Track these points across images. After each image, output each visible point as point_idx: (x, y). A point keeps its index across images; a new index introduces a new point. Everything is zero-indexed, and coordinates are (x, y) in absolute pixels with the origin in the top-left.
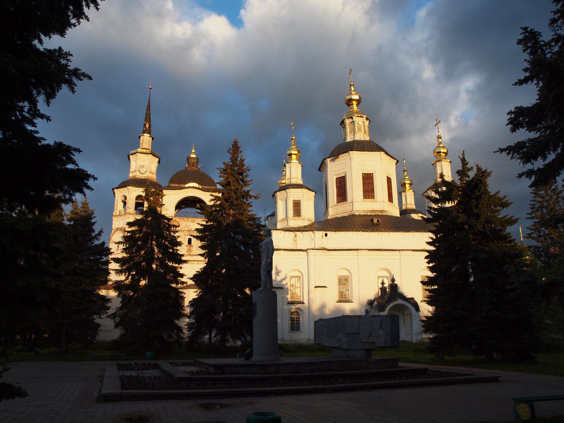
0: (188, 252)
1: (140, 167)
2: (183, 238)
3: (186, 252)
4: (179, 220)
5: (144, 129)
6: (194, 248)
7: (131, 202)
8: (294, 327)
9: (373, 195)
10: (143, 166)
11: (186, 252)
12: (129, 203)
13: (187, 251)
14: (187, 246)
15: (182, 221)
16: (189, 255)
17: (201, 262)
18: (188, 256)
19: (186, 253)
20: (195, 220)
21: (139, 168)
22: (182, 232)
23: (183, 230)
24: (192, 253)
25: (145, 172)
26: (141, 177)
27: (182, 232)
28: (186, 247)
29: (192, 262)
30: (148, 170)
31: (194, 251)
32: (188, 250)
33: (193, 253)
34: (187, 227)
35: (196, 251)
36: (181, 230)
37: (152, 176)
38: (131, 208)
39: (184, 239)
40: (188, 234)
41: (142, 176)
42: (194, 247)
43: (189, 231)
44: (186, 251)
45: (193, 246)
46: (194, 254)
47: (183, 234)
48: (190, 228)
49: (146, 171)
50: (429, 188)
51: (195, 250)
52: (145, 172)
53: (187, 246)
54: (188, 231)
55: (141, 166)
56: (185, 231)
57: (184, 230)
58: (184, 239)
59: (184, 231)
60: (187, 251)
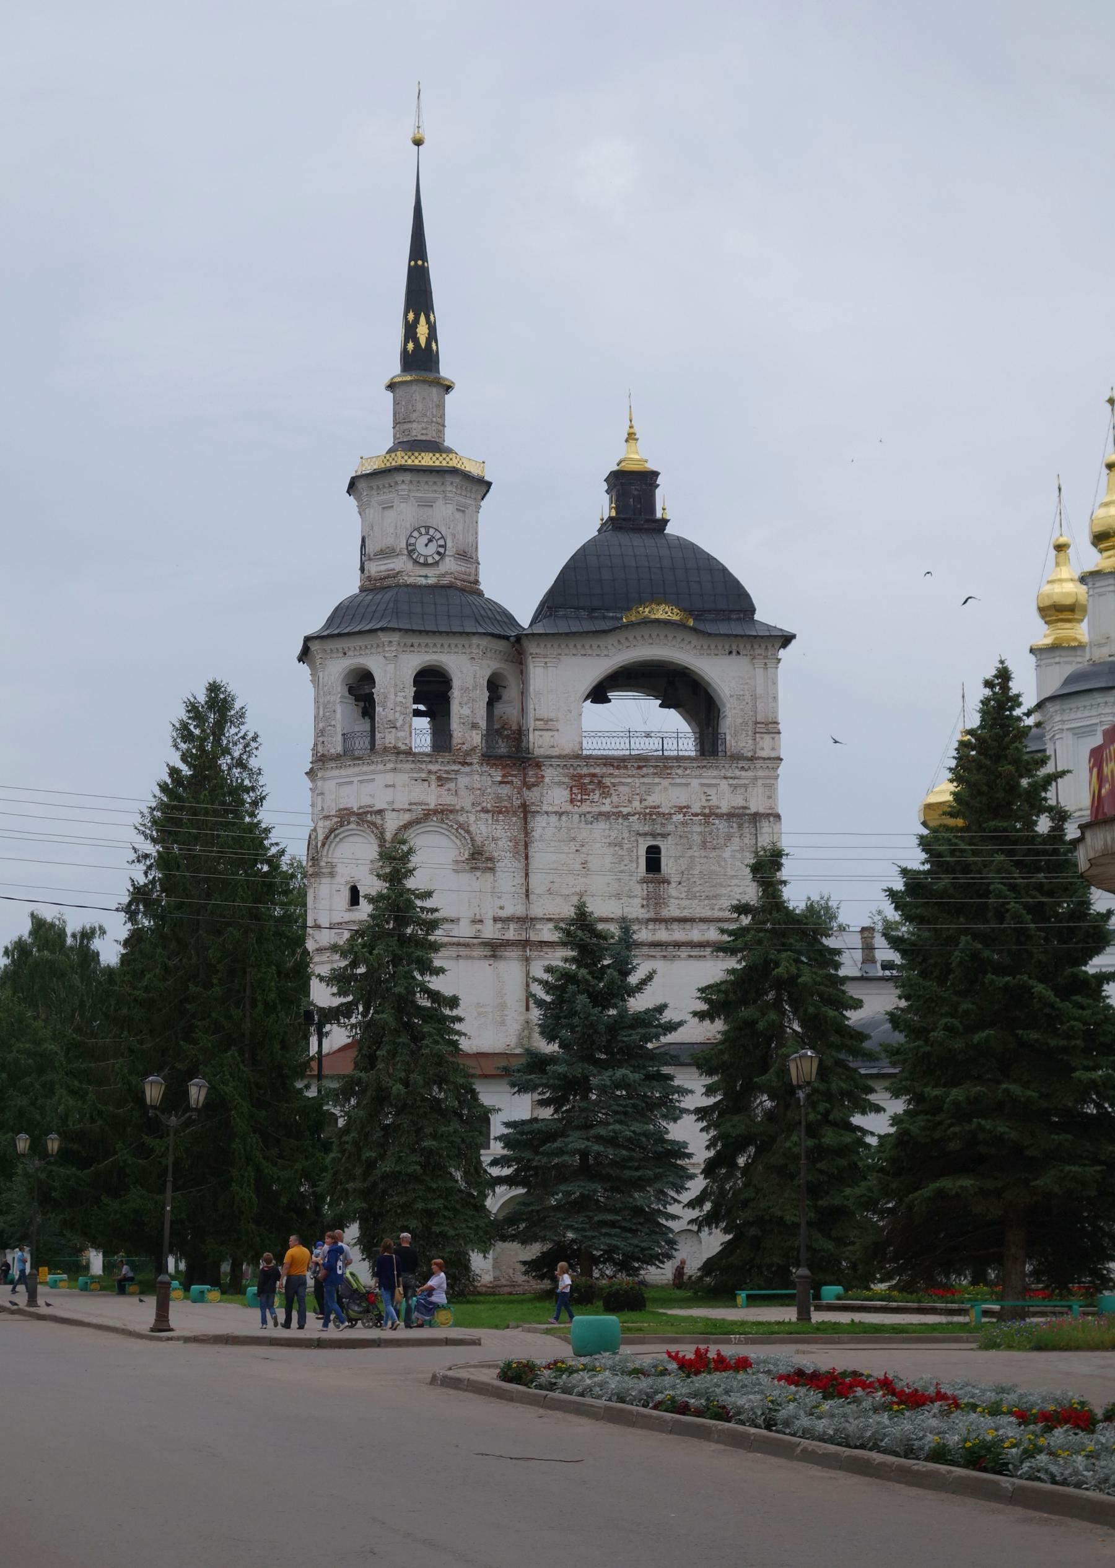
0: (648, 906)
1: (416, 534)
2: (626, 847)
3: (643, 906)
4: (604, 770)
5: (410, 346)
6: (672, 890)
7: (399, 699)
10: (427, 528)
11: (643, 906)
12: (390, 705)
13: (645, 903)
14: (644, 881)
15: (616, 772)
19: (643, 910)
20: (671, 767)
21: (412, 541)
22: (620, 821)
23: (625, 811)
24: (666, 913)
25: (437, 557)
26: (423, 581)
27: (620, 821)
28: (639, 887)
29: (670, 949)
30: (449, 544)
32: (648, 899)
33: (672, 910)
35: (686, 903)
36: (614, 814)
37: (463, 569)
38: (398, 725)
39: (630, 850)
40: (647, 829)
41: (426, 577)
42: (673, 885)
45: (669, 883)
46: (676, 913)
48: (652, 800)
49: (442, 550)
52: (439, 553)
53: (644, 881)
54: (646, 814)
55: (418, 529)
57: (629, 814)
58: (630, 850)
59: (626, 817)
60: (645, 903)
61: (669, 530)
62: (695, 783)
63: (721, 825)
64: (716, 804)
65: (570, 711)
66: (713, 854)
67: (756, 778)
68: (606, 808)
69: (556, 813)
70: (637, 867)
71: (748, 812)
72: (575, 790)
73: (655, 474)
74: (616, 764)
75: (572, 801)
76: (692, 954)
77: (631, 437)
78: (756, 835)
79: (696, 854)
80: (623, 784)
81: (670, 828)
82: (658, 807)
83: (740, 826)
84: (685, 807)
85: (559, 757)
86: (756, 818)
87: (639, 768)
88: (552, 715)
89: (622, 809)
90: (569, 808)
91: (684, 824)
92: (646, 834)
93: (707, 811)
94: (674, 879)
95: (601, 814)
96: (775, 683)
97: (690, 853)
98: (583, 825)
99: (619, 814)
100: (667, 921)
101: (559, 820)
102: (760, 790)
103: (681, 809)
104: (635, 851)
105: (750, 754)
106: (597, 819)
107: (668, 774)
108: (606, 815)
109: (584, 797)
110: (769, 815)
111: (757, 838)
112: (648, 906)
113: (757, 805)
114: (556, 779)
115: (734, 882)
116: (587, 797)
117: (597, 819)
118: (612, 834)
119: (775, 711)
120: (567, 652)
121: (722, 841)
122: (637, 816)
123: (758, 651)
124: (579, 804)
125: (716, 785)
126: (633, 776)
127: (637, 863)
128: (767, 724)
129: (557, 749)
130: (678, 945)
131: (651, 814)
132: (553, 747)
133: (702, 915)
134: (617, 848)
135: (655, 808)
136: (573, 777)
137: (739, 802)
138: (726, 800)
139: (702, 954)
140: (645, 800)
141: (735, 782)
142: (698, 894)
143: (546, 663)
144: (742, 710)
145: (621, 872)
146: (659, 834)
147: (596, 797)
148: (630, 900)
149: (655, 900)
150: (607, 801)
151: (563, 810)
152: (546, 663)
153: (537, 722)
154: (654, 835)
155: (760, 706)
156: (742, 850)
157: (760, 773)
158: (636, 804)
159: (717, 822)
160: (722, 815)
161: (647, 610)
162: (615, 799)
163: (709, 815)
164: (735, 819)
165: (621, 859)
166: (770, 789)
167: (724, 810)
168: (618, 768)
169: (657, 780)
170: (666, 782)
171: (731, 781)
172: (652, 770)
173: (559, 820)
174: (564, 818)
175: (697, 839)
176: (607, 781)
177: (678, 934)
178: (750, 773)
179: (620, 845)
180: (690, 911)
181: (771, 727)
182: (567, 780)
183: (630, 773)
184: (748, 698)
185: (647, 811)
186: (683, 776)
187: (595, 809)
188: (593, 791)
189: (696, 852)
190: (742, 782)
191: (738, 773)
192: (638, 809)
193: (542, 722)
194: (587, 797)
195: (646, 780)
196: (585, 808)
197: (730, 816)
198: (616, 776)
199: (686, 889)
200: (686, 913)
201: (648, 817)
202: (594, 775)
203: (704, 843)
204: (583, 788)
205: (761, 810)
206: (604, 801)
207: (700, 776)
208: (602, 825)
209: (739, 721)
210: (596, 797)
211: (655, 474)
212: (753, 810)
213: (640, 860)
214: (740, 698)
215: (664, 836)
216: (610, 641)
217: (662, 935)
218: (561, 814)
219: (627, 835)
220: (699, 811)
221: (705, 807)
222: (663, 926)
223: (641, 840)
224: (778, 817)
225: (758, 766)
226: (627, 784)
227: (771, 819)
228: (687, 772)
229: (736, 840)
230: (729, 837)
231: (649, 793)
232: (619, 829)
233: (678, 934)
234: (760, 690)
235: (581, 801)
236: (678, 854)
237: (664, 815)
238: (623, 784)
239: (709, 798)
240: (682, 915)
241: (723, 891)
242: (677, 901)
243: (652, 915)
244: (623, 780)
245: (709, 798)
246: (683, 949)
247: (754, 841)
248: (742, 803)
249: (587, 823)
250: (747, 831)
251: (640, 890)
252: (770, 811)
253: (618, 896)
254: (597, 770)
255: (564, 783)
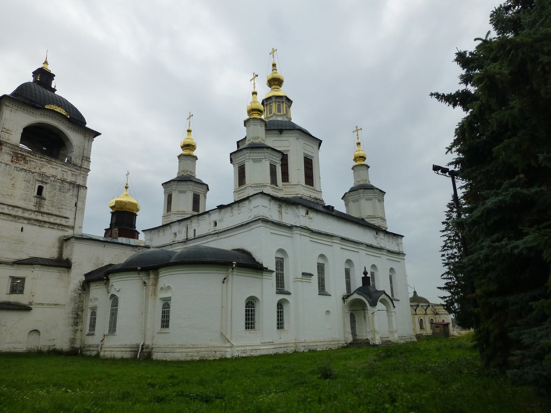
0: (36, 206)
2: (31, 183)
3: (34, 206)
4: (27, 154)
6: (46, 202)
8: (249, 323)
9: (312, 181)
11: (34, 206)
13: (35, 204)
14: (35, 197)
15: (32, 156)
16: (38, 212)
17: (56, 226)
18: (36, 213)
19: (34, 207)
22: (30, 173)
23: (33, 171)
24: (42, 210)
27: (30, 173)
28: (34, 198)
31: (45, 206)
32: (36, 204)
33: (44, 210)
34: (38, 168)
36: (28, 170)
39: (32, 185)
40: (40, 179)
43: (42, 175)
44: (32, 204)
45: (45, 200)
46: (46, 211)
47: (32, 177)
48: (43, 170)
50: (351, 188)
51: (48, 206)
53: (35, 197)
54: (40, 174)
56: (36, 173)
57: (34, 172)
59: (33, 173)
60: (35, 204)
61: (56, 93)
62: (60, 169)
63: (67, 186)
64: (66, 178)
65: (17, 130)
66: (63, 194)
67: (81, 174)
68: (26, 168)
69: (5, 164)
70: (34, 191)
71: (76, 183)
72: (14, 158)
73: (54, 75)
74: (32, 154)
75: (12, 161)
76: (50, 226)
77: (46, 63)
78: (78, 191)
79: (56, 192)
80: (33, 161)
81: (49, 181)
82: (45, 173)
83: (73, 187)
84: (55, 176)
85: (10, 144)
86: (79, 186)
87: (41, 158)
88: (10, 129)
89: (32, 170)
90: (11, 163)
91: (54, 181)
92: (39, 181)
93: (62, 179)
94: (47, 198)
95: (23, 169)
96: (91, 146)
97: (55, 191)
98: (15, 171)
99: (30, 171)
100: (43, 213)
101: (6, 166)
102: (82, 178)
103: (53, 176)
104: (34, 186)
105: (80, 166)
106: (21, 170)
107: (51, 163)
108: (26, 170)
109: (17, 161)
110: (83, 186)
111: (78, 193)
112: (36, 206)
113: (79, 182)
114: (7, 152)
115: (69, 205)
116: (18, 162)
117: (21, 170)
118: (26, 177)
119: (90, 155)
120: (20, 110)
121: (66, 190)
122: (37, 174)
123: (87, 135)
124: (15, 163)
125: (67, 172)
126: (38, 160)
127: (35, 190)
128: (87, 158)
129: (10, 141)
130: (45, 222)
131: (42, 175)
132: (9, 140)
133: (56, 214)
134: (27, 183)
135: (44, 173)
136: (14, 153)
137: (73, 179)
138: (70, 178)
139: (53, 227)
140: (41, 169)
141: (73, 173)
142: (55, 206)
143: (11, 110)
144: (79, 151)
145: (27, 191)
146: (44, 182)
147: (22, 163)
148: (29, 202)
149: (39, 204)
150: (27, 165)
151: (8, 163)
152: (11, 110)
153: (3, 129)
154: (42, 182)
155: (85, 152)
156: (73, 195)
157: (82, 172)
158: (37, 170)
159: (66, 184)
160: (68, 182)
161: (54, 107)
162: (29, 165)
163: (63, 181)
164: (72, 185)
165: (28, 187)
166: (85, 178)
167: (68, 181)
168: (33, 155)
169: (46, 164)
170: (49, 166)
171: (72, 172)
172: (45, 160)
173: (6, 166)
174: (8, 166)
175: (58, 188)
176: (28, 159)
177: (46, 218)
178: (78, 171)
179: (29, 183)
180: (52, 211)
181: (88, 159)
182: (11, 153)
183: (37, 158)
184: (81, 148)
185: (41, 173)
186: (56, 165)
187: (21, 167)
188: (21, 160)
189: (57, 192)
190: (75, 173)
191: (74, 170)
192: (38, 172)
193: (6, 130)
194: (18, 162)
195: (42, 163)
196: (17, 165)
197: (70, 183)
198: (31, 158)
199: (51, 203)
200: (49, 212)
201: (41, 175)
202: (23, 155)
203: (60, 189)
204: (17, 157)
205: (81, 184)
206: (25, 165)
207: (62, 167)
208: (22, 173)
209: (78, 154)
210: (22, 163)
211: (54, 75)
212: (78, 183)
213: (35, 189)
214: (79, 147)
215: (46, 183)
216: (38, 112)
217: (40, 217)
218: (7, 164)
219: (32, 179)
220: (60, 179)
221: (62, 178)
222: (40, 214)
223: (37, 182)
224: (86, 188)
225: (82, 170)
226: (35, 162)
227: (84, 188)
228: (58, 165)
229: (71, 191)
230: (69, 190)
231: (42, 167)
232: (29, 176)
233: (46, 218)
234: (86, 147)
235: (16, 162)
236: (51, 191)
237: (47, 176)
238: (33, 161)
239: (63, 175)
240: (48, 212)
241: (64, 207)
242: (47, 207)
243: (37, 209)
244: (34, 160)
245: (63, 175)
246: (47, 224)
247: (77, 193)
248: (74, 180)
249: (17, 170)
250: (76, 190)
251: (34, 200)
252: (83, 185)
253: (25, 200)
254: (24, 154)
255: (10, 154)
